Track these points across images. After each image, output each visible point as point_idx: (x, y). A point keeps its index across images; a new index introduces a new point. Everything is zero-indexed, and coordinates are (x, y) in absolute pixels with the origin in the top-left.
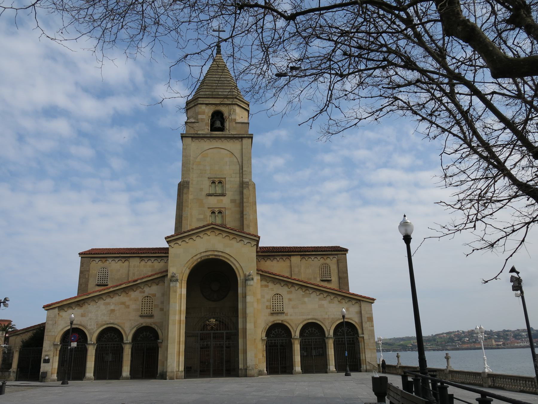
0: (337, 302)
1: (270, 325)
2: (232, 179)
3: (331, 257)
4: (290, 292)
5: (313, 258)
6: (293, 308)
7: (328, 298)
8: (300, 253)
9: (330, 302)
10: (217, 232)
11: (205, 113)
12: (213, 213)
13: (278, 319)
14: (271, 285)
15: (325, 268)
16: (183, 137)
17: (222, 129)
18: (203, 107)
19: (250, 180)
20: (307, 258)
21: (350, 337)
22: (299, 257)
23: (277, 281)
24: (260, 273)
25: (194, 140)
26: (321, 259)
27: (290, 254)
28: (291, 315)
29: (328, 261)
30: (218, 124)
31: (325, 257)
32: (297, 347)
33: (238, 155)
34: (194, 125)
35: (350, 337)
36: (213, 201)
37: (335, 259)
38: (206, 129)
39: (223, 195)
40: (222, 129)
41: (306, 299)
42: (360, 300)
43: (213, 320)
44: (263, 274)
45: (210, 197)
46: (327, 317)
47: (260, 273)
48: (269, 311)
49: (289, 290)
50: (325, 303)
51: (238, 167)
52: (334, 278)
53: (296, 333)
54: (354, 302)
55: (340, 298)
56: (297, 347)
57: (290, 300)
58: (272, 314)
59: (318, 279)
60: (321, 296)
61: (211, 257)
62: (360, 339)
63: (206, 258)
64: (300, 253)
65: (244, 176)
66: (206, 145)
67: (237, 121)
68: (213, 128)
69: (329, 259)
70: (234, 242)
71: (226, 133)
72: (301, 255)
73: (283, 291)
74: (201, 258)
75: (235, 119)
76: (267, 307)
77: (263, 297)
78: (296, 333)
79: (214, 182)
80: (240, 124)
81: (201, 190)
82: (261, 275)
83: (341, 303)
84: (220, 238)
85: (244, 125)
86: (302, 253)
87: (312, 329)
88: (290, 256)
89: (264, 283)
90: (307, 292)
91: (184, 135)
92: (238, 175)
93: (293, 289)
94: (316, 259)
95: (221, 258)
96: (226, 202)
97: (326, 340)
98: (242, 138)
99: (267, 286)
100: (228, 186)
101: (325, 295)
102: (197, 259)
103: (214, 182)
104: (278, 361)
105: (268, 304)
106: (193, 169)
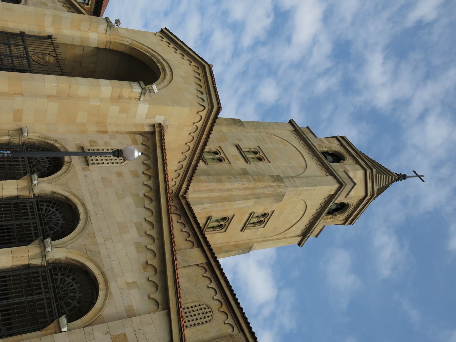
0: (143, 260)
1: (57, 145)
3: (230, 320)
4: (135, 174)
5: (213, 285)
6: (104, 179)
8: (211, 260)
9: (137, 245)
18: (336, 142)
20: (208, 274)
21: (54, 305)
22: (204, 260)
23: (151, 155)
24: (157, 130)
25: (294, 132)
26: (217, 303)
27: (203, 244)
28: (86, 176)
29: (219, 317)
31: (224, 308)
35: (54, 305)
37: (230, 330)
41: (129, 200)
42: (167, 307)
44: (157, 134)
45: (235, 148)
46: (100, 240)
47: (157, 130)
49: (140, 173)
50: (133, 234)
54: (157, 296)
55: (155, 262)
57: (120, 175)
61: (159, 65)
62: (52, 326)
63: (155, 61)
64: (211, 260)
69: (224, 317)
72: (209, 263)
74: (153, 55)
79: (256, 153)
82: (153, 133)
83: (144, 269)
86: (213, 263)
88: (200, 245)
90: (147, 202)
91: (293, 122)
93: (144, 179)
94: (212, 292)
95: (162, 74)
97: (37, 242)
101: (153, 233)
102: (149, 52)
106: (260, 132)
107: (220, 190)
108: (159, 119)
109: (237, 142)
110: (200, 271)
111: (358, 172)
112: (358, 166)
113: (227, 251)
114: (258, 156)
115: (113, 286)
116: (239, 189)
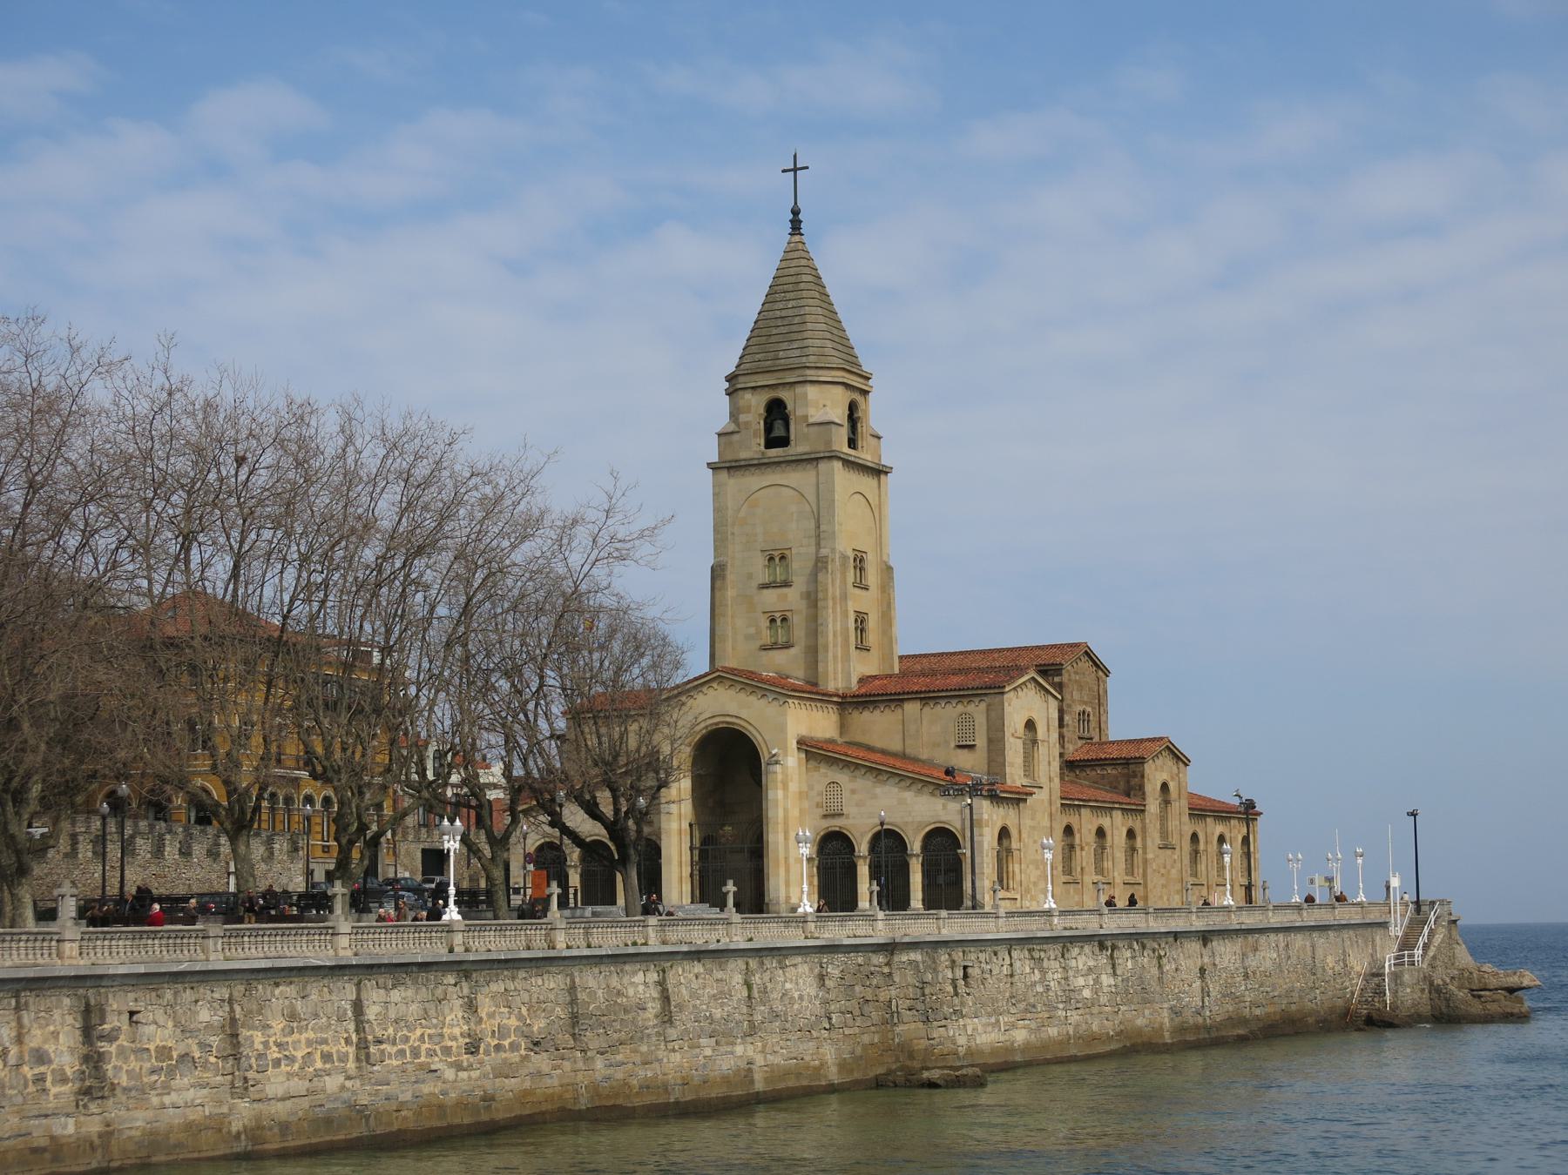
2: (803, 550)
3: (976, 700)
7: (914, 787)
10: (729, 683)
11: (756, 404)
12: (773, 621)
13: (835, 824)
14: (824, 769)
15: (966, 721)
16: (714, 467)
17: (784, 442)
18: (748, 396)
19: (833, 550)
29: (971, 708)
30: (779, 431)
32: (863, 871)
33: (812, 498)
34: (736, 437)
36: (771, 598)
38: (754, 446)
39: (786, 584)
40: (784, 442)
43: (728, 828)
45: (765, 591)
48: (821, 811)
50: (909, 795)
51: (812, 525)
52: (981, 741)
56: (863, 871)
57: (853, 792)
58: (825, 816)
59: (953, 745)
60: (903, 784)
65: (823, 543)
66: (754, 481)
67: (811, 420)
70: (753, 698)
71: (797, 448)
73: (842, 777)
75: (806, 417)
76: (817, 806)
77: (811, 788)
78: (862, 848)
80: (816, 428)
81: (750, 576)
84: (731, 692)
85: (822, 428)
87: (888, 842)
88: (902, 700)
89: (812, 764)
92: (813, 541)
96: (792, 599)
98: (817, 459)
99: (817, 769)
100: (795, 565)
103: (771, 559)
104: (836, 892)
105: (818, 799)
107: (835, 646)
108: (795, 745)
109: (755, 584)
110: (927, 709)
111: (810, 396)
112: (799, 389)
113: (889, 605)
114: (777, 558)
115: (943, 819)
116: (835, 621)
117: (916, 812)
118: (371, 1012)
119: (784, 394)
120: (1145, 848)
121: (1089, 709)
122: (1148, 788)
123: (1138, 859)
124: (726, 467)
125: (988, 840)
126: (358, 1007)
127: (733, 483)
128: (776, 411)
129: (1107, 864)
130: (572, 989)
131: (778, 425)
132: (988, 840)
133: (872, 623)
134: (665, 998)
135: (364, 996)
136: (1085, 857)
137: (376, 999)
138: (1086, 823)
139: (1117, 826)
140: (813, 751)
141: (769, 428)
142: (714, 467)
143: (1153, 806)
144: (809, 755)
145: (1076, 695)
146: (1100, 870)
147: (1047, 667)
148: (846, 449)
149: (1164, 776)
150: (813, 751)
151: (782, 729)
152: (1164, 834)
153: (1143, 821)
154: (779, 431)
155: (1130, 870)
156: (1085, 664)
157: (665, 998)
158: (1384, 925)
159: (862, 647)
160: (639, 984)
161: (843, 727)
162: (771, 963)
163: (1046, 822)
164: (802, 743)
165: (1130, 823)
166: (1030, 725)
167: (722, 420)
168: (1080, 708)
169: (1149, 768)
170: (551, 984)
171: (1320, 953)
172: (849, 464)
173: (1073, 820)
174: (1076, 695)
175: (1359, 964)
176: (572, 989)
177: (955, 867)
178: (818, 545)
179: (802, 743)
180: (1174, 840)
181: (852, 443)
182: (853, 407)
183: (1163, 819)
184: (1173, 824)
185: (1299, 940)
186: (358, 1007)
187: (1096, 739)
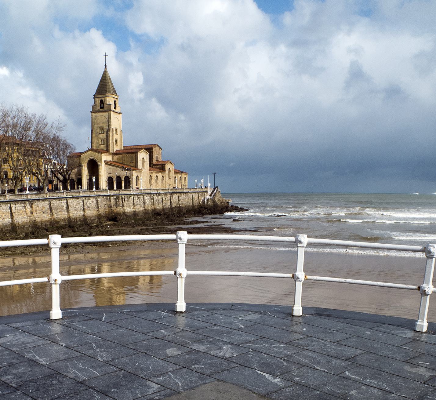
2: (106, 128)
13: (110, 175)
14: (108, 166)
16: (90, 112)
30: (102, 106)
34: (95, 106)
48: (108, 173)
53: (115, 179)
58: (109, 174)
66: (98, 114)
67: (107, 104)
68: (101, 108)
87: (119, 179)
89: (106, 165)
99: (107, 166)
104: (111, 187)
108: (104, 162)
109: (98, 134)
117: (123, 174)
118: (13, 208)
119: (103, 99)
120: (165, 179)
121: (158, 156)
122: (166, 169)
123: (164, 181)
124: (94, 111)
125: (134, 178)
126: (10, 208)
127: (94, 114)
128: (102, 102)
129: (158, 182)
130: (50, 204)
131: (102, 104)
132: (134, 178)
133: (119, 141)
134: (68, 205)
135: (11, 206)
136: (154, 181)
137: (13, 206)
138: (154, 175)
139: (160, 175)
140: (107, 163)
141: (100, 105)
142: (91, 112)
143: (167, 172)
144: (106, 164)
145: (155, 153)
146: (156, 182)
147: (149, 150)
148: (114, 109)
149: (170, 167)
150: (107, 163)
151: (101, 159)
152: (169, 176)
153: (165, 174)
154: (102, 106)
155: (162, 182)
156: (157, 148)
157: (68, 205)
158: (207, 192)
159: (117, 145)
160: (64, 202)
161: (113, 159)
162: (87, 199)
163: (146, 175)
164: (105, 161)
165: (163, 175)
166: (143, 158)
167: (93, 103)
168: (156, 155)
169: (166, 166)
170: (47, 203)
171: (193, 196)
172: (113, 111)
173: (152, 175)
174: (155, 153)
175: (202, 199)
176: (50, 204)
177: (129, 182)
178: (108, 127)
179: (105, 161)
180: (171, 177)
181: (115, 108)
182: (115, 101)
183: (169, 174)
184: (171, 175)
185: (190, 195)
186: (10, 208)
187: (159, 161)
